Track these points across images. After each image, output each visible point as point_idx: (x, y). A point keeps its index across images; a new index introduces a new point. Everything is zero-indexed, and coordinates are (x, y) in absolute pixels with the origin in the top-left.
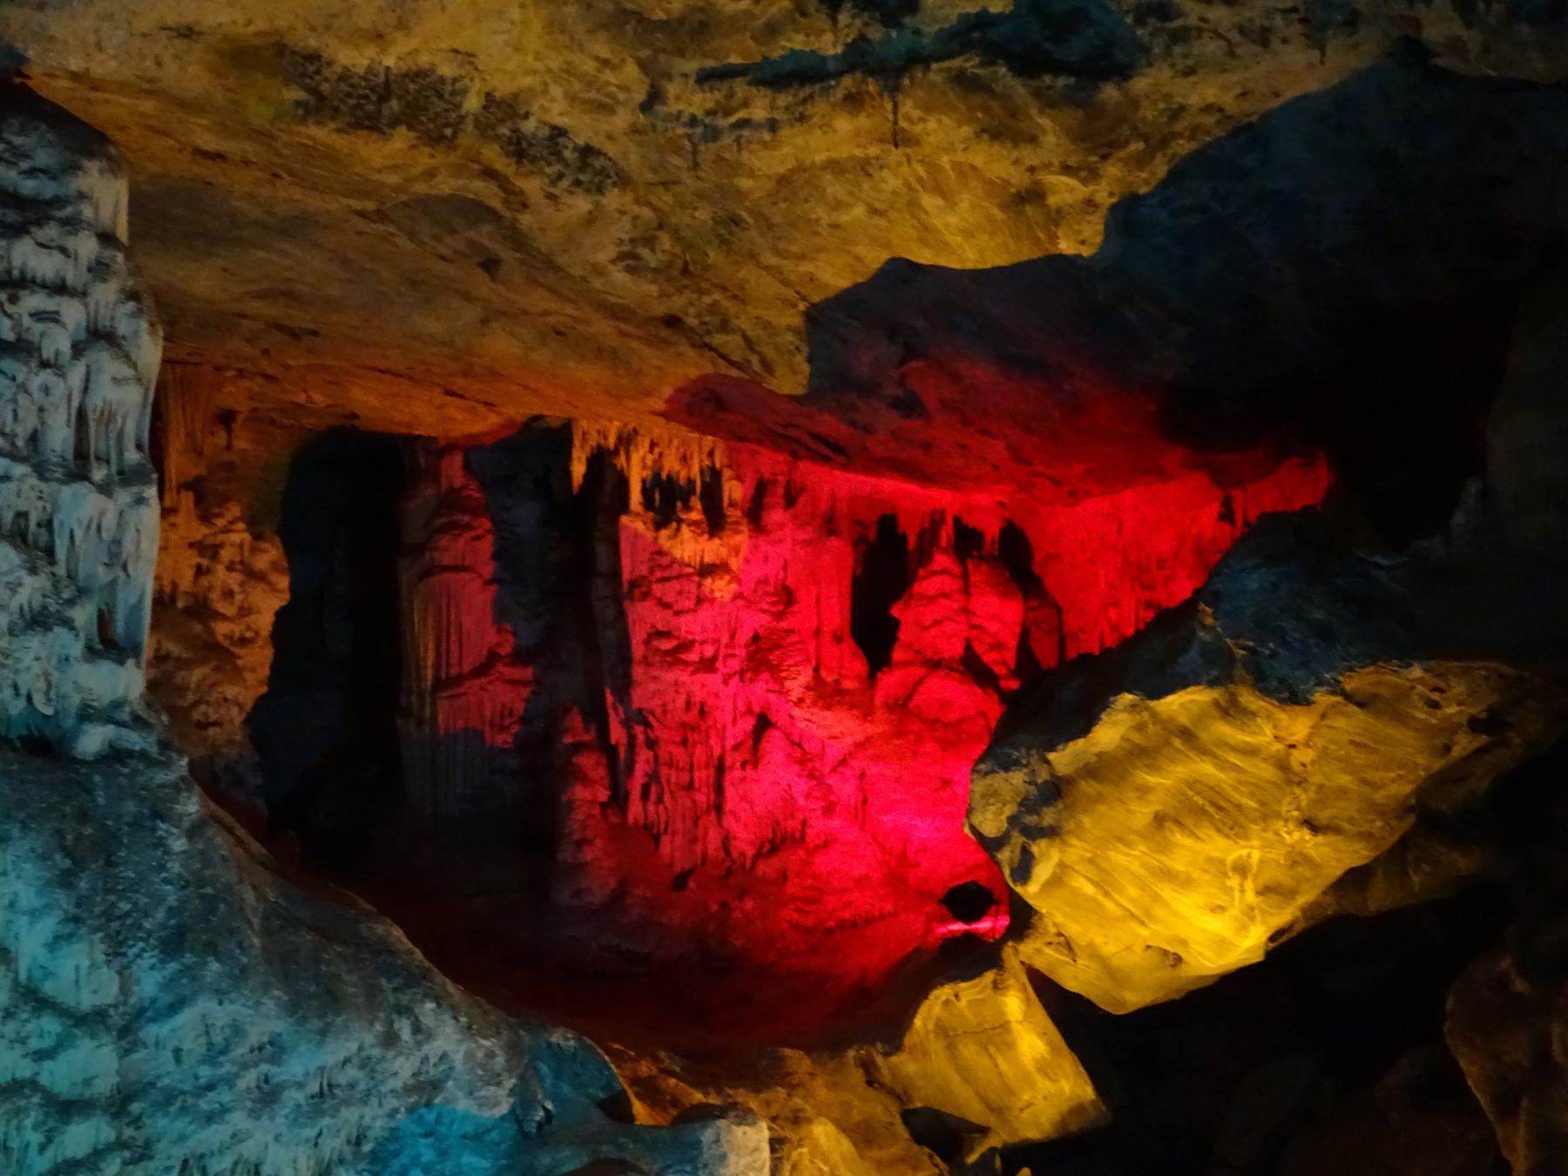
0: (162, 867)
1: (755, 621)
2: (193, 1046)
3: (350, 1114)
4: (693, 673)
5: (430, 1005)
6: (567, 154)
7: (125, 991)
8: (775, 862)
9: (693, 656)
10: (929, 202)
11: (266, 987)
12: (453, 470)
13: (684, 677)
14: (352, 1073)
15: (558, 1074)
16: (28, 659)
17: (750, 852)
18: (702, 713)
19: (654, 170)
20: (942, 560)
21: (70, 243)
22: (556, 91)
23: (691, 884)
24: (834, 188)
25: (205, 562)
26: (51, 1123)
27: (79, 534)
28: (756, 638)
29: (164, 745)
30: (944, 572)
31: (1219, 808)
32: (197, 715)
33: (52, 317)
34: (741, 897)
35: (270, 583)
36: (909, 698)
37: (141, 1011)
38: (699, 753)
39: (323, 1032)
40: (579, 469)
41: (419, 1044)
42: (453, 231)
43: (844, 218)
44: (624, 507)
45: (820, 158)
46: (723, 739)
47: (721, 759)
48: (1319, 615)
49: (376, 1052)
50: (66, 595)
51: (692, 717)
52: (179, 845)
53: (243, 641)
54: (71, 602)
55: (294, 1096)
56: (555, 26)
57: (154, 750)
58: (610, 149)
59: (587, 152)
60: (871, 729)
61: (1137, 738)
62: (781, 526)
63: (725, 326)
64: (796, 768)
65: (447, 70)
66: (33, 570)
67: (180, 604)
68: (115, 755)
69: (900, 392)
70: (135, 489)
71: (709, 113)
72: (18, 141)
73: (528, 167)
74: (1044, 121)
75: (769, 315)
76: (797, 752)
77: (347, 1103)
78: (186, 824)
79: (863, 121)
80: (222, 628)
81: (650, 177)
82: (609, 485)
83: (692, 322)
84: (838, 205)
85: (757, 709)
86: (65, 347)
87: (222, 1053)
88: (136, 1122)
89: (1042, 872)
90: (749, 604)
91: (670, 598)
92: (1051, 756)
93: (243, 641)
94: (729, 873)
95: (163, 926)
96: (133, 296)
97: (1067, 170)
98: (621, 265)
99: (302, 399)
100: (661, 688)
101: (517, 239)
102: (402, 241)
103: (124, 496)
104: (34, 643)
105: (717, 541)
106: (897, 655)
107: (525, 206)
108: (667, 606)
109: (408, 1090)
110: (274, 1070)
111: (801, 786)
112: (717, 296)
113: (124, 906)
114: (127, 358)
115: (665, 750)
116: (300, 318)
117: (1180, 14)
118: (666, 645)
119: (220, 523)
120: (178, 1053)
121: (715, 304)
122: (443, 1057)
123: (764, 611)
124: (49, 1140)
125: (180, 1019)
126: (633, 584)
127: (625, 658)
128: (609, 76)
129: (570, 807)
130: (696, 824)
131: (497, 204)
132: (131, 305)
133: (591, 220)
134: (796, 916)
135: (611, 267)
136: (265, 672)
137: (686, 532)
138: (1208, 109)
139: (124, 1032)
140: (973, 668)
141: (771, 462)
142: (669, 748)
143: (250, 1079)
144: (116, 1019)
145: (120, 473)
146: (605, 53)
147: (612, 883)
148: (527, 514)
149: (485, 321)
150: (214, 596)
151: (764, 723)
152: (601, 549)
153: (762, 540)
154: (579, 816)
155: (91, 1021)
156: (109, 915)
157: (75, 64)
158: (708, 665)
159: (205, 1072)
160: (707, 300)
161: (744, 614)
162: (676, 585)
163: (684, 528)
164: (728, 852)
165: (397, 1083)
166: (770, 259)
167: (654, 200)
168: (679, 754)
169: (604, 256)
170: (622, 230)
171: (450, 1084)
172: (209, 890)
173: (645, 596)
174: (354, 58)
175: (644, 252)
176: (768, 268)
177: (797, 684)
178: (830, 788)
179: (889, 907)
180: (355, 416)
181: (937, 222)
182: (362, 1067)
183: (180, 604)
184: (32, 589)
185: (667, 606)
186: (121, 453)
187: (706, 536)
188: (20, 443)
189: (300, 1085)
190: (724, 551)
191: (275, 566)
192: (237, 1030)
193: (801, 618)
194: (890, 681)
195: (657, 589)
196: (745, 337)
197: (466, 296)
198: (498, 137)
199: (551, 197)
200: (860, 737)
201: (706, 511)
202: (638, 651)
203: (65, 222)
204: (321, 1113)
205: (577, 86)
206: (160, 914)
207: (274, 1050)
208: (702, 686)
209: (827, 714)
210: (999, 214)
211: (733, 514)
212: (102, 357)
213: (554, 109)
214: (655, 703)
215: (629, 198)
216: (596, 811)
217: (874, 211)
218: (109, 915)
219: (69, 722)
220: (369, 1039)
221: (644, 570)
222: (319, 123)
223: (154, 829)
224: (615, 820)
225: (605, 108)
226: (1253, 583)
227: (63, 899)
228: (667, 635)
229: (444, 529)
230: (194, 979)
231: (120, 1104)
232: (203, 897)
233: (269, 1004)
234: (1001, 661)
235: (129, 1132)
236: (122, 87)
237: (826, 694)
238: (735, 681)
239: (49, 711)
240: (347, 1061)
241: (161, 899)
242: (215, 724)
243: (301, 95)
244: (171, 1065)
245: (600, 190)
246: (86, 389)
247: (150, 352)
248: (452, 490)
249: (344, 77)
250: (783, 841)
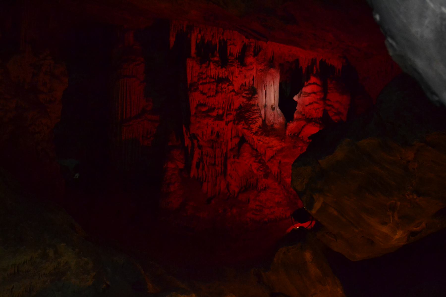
9: (214, 114)
18: (218, 135)
20: (313, 79)
30: (314, 83)
36: (300, 133)
40: (172, 40)
85: (240, 135)
89: (318, 205)
92: (320, 161)
106: (295, 116)
118: (204, 109)
123: (243, 97)
137: (212, 66)
158: (220, 118)
163: (211, 64)
187: (220, 67)
202: (193, 111)
209: (267, 138)
228: (205, 105)
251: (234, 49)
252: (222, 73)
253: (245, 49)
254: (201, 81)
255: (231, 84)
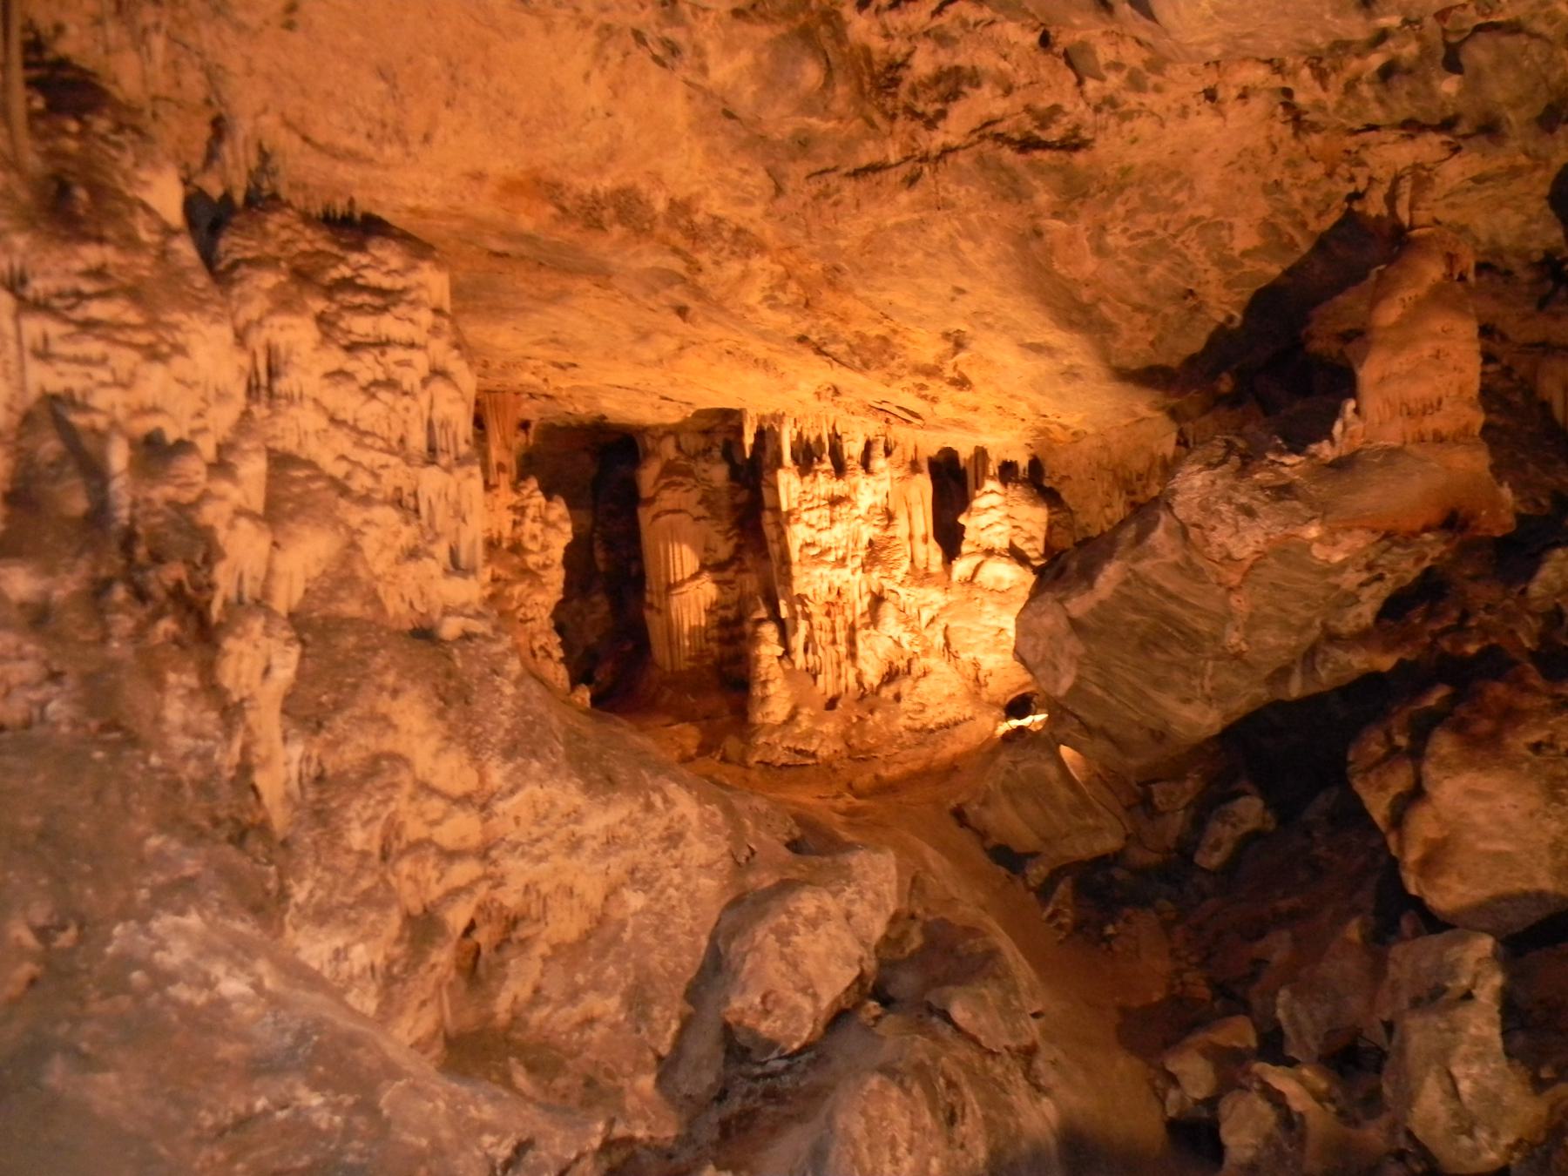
0: (500, 704)
1: (868, 532)
2: (527, 814)
3: (627, 854)
4: (834, 568)
5: (673, 785)
6: (726, 234)
7: (482, 779)
8: (893, 688)
9: (831, 558)
10: (965, 245)
11: (569, 776)
12: (669, 449)
13: (824, 570)
14: (625, 829)
15: (757, 825)
16: (409, 579)
17: (876, 682)
19: (782, 240)
20: (991, 485)
21: (416, 316)
22: (714, 193)
23: (840, 705)
24: (901, 242)
25: (518, 518)
26: (443, 864)
27: (434, 500)
28: (871, 543)
29: (496, 629)
31: (1181, 632)
32: (519, 615)
33: (406, 364)
34: (871, 712)
35: (560, 529)
36: (974, 576)
37: (493, 794)
38: (839, 621)
39: (607, 804)
40: (749, 439)
41: (667, 809)
42: (656, 292)
43: (909, 262)
44: (779, 463)
45: (890, 222)
46: (853, 608)
47: (853, 623)
48: (1243, 500)
49: (640, 815)
50: (429, 537)
51: (832, 597)
52: (509, 690)
53: (545, 567)
54: (431, 542)
55: (591, 844)
56: (711, 150)
57: (490, 633)
58: (753, 229)
59: (739, 231)
60: (951, 598)
61: (1125, 590)
62: (882, 470)
63: (835, 338)
64: (902, 627)
65: (643, 186)
66: (407, 523)
67: (505, 545)
68: (467, 636)
69: (956, 375)
70: (467, 468)
71: (815, 198)
72: (378, 253)
73: (699, 245)
74: (1037, 183)
75: (864, 330)
76: (903, 617)
77: (624, 848)
78: (513, 677)
79: (917, 193)
80: (532, 560)
81: (779, 244)
82: (770, 449)
83: (814, 337)
84: (904, 253)
86: (417, 383)
87: (546, 817)
88: (494, 863)
90: (866, 521)
91: (813, 521)
93: (545, 567)
94: (863, 696)
95: (502, 741)
96: (457, 346)
97: (1056, 215)
98: (765, 305)
99: (571, 409)
100: (812, 581)
101: (699, 294)
102: (624, 300)
103: (459, 473)
104: (412, 567)
105: (841, 482)
106: (965, 548)
107: (700, 270)
108: (812, 526)
109: (662, 839)
110: (577, 828)
111: (906, 638)
112: (829, 320)
113: (478, 729)
114: (456, 386)
115: (816, 621)
116: (565, 358)
117: (1126, 102)
119: (525, 492)
120: (517, 820)
121: (828, 325)
122: (683, 817)
124: (442, 875)
125: (519, 797)
126: (789, 513)
127: (785, 560)
128: (747, 180)
129: (758, 659)
130: (839, 664)
131: (682, 271)
132: (456, 353)
133: (745, 276)
134: (909, 723)
135: (759, 307)
136: (560, 585)
138: (1149, 165)
139: (484, 807)
140: (1016, 555)
141: (873, 427)
142: (819, 618)
143: (562, 834)
144: (479, 801)
145: (457, 459)
146: (745, 166)
147: (788, 707)
148: (719, 474)
149: (681, 348)
150: (526, 539)
151: (878, 600)
152: (766, 492)
153: (871, 480)
154: (764, 664)
155: (465, 800)
156: (469, 736)
157: (410, 202)
158: (841, 563)
159: (536, 832)
160: (823, 323)
161: (863, 528)
162: (816, 513)
164: (860, 684)
165: (655, 835)
166: (860, 292)
167: (783, 259)
168: (826, 621)
169: (754, 297)
170: (762, 281)
171: (690, 835)
172: (530, 718)
173: (798, 520)
174: (585, 185)
175: (779, 295)
176: (861, 299)
177: (899, 574)
178: (925, 639)
179: (968, 713)
180: (604, 417)
181: (971, 258)
182: (632, 824)
183: (505, 545)
184: (408, 535)
185: (812, 526)
186: (456, 444)
188: (394, 443)
189: (594, 837)
190: (847, 489)
191: (561, 516)
192: (553, 804)
193: (901, 529)
194: (961, 567)
195: (805, 516)
196: (850, 346)
197: (668, 333)
198: (679, 227)
199: (717, 263)
200: (943, 604)
201: (833, 463)
202: (795, 556)
203: (412, 303)
204: (607, 855)
205: (728, 189)
206: (501, 733)
207: (576, 816)
208: (841, 577)
210: (1011, 249)
211: (851, 464)
212: (438, 386)
213: (715, 204)
214: (809, 592)
215: (767, 260)
216: (776, 661)
217: (928, 255)
218: (469, 736)
219: (436, 617)
220: (636, 808)
221: (795, 505)
222: (565, 228)
223: (492, 682)
224: (788, 667)
225: (747, 202)
226: (1197, 481)
227: (440, 726)
228: (813, 544)
229: (667, 486)
230: (524, 773)
231: (483, 853)
232: (526, 723)
233: (572, 788)
234: (1034, 550)
235: (491, 869)
236: (442, 215)
237: (920, 576)
238: (859, 572)
239: (423, 610)
240: (622, 821)
241: (499, 724)
242: (533, 619)
243: (551, 210)
244: (512, 826)
245: (748, 256)
246: (431, 407)
247: (469, 382)
248: (669, 461)
249: (580, 197)
250: (897, 672)
251: (853, 448)
252: (839, 487)
253: (869, 445)
254: (805, 506)
255: (854, 506)
